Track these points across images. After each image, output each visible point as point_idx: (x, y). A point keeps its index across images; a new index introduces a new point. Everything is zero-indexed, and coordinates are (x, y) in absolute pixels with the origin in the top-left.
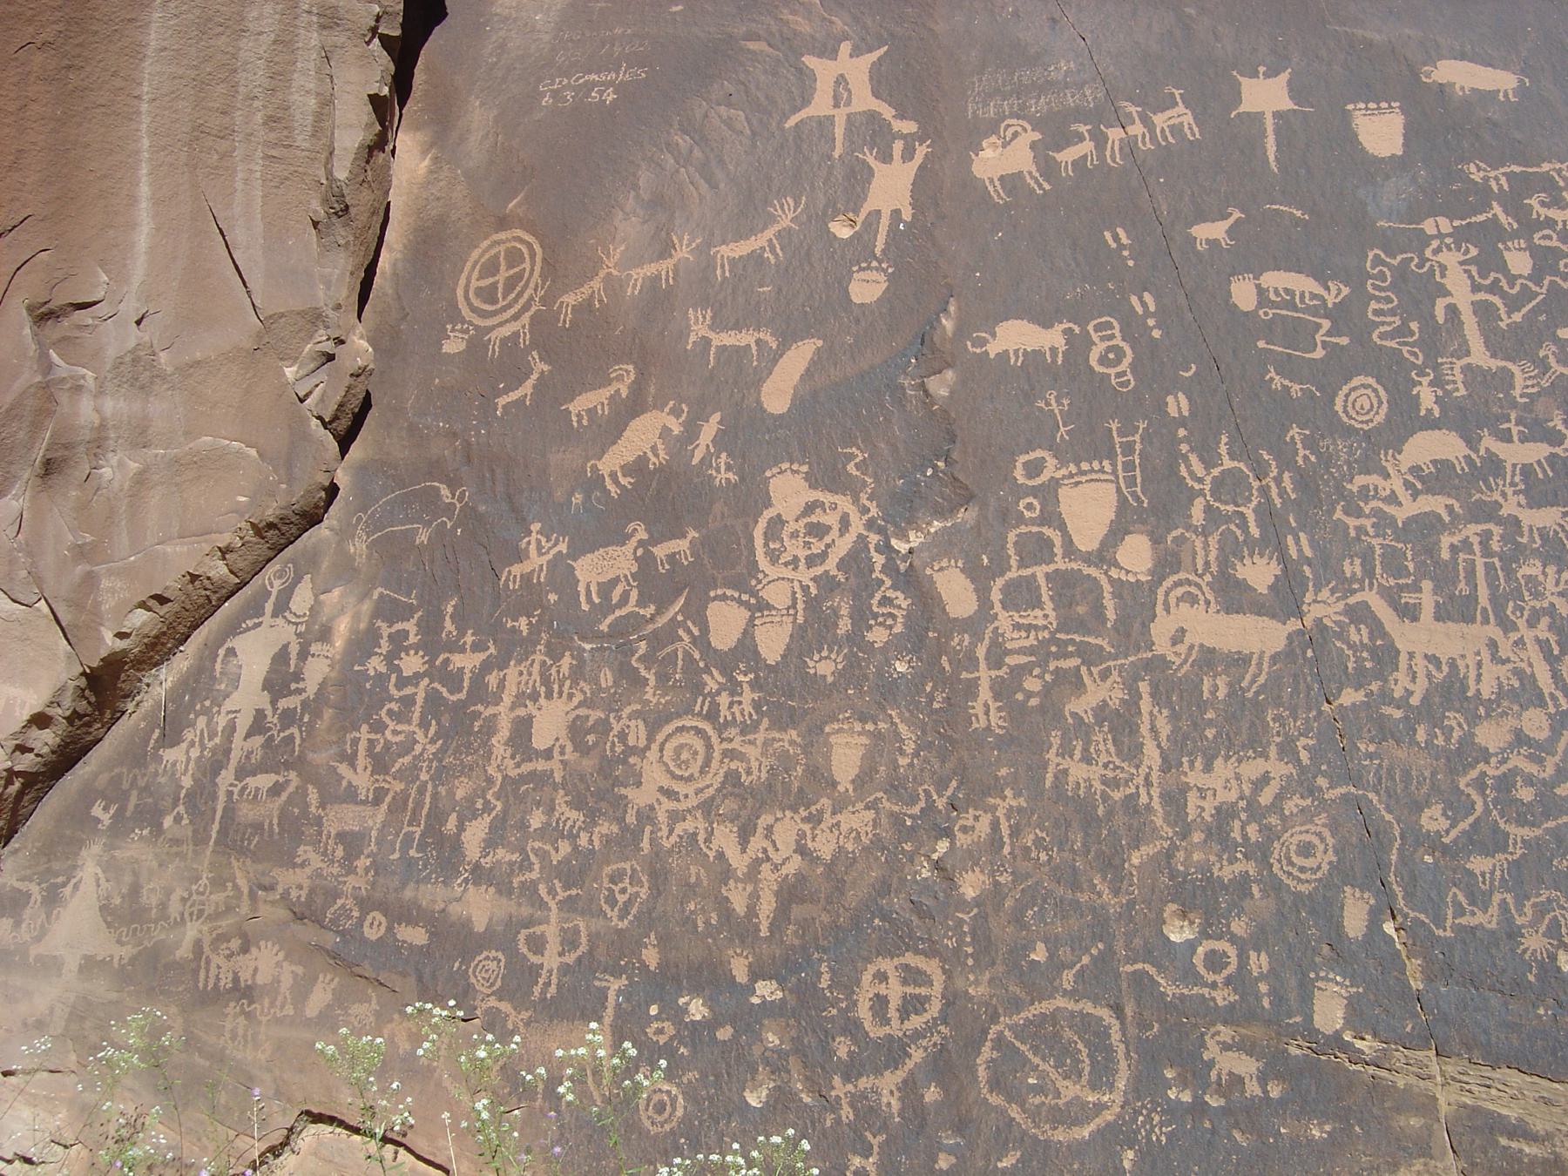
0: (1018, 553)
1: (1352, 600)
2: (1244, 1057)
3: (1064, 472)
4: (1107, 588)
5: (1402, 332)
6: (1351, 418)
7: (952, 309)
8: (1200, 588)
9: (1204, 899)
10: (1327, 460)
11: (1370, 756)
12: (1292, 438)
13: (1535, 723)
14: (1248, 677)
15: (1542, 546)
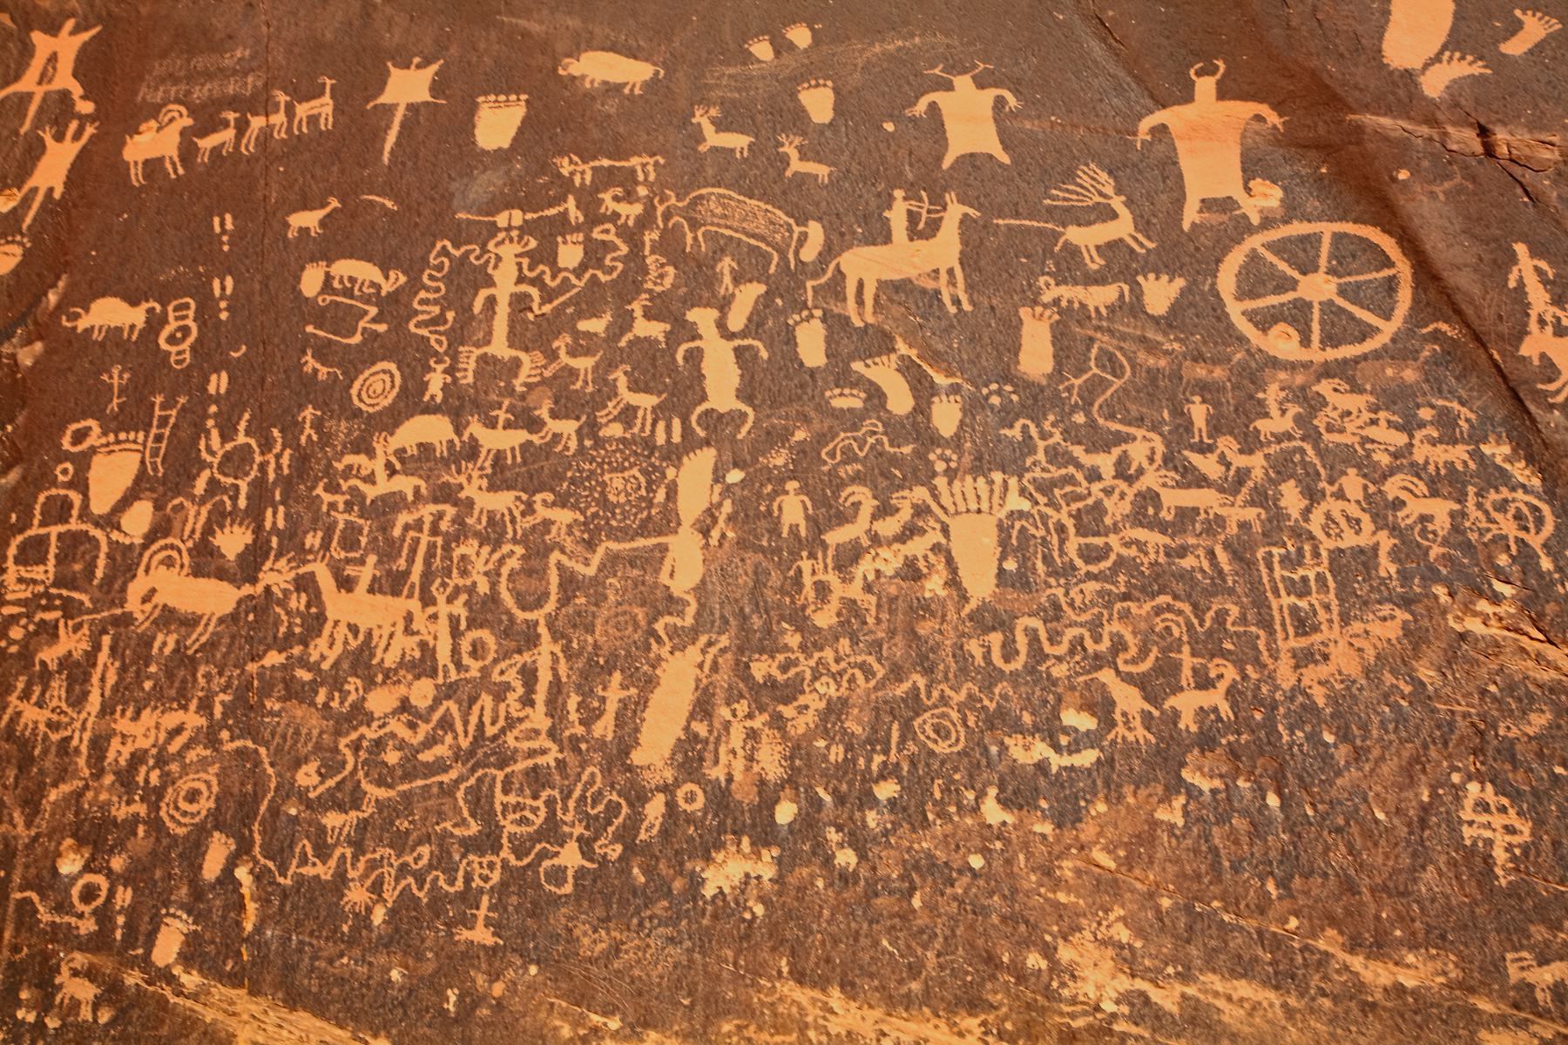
0: (42, 513)
1: (301, 571)
2: (87, 983)
3: (103, 441)
4: (104, 548)
5: (439, 320)
6: (361, 400)
7: (61, 284)
8: (180, 552)
9: (97, 836)
10: (326, 438)
11: (272, 713)
13: (422, 692)
14: (194, 636)
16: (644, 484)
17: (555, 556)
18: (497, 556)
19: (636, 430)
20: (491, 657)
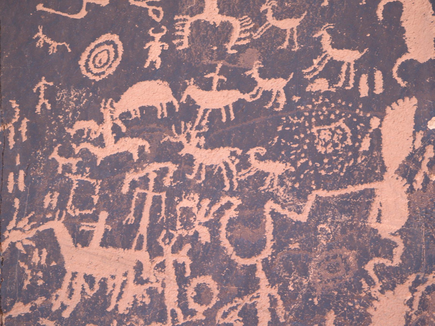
1: (41, 229)
6: (88, 70)
10: (57, 107)
12: (39, 89)
15: (204, 182)
16: (349, 134)
17: (269, 205)
18: (216, 208)
19: (340, 84)
20: (214, 301)
